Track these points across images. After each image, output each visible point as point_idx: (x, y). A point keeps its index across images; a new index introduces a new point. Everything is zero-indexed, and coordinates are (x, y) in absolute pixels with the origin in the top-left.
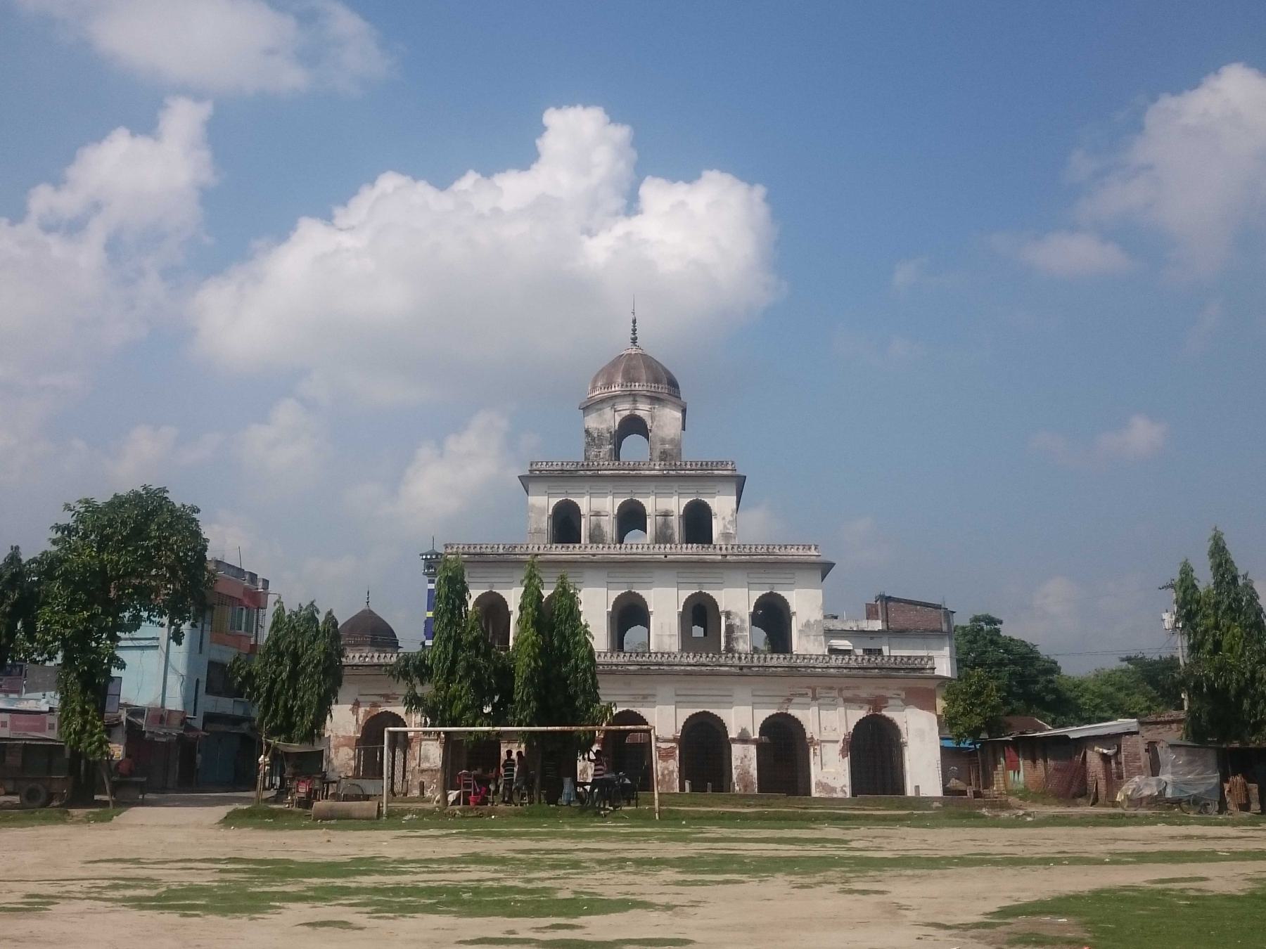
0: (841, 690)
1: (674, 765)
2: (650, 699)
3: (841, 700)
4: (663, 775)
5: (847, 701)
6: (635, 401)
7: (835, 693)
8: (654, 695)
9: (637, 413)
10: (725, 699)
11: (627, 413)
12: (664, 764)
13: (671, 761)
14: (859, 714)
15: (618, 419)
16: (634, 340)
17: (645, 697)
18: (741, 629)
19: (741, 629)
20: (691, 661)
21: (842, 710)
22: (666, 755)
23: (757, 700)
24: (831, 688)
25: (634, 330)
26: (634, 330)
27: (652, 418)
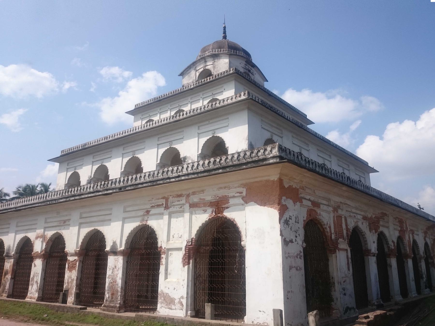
0: (188, 196)
2: (67, 223)
5: (193, 206)
6: (206, 62)
8: (69, 220)
9: (207, 68)
11: (202, 69)
15: (198, 74)
16: (225, 37)
21: (187, 215)
23: (127, 215)
24: (180, 196)
25: (225, 33)
26: (225, 33)
27: (214, 67)
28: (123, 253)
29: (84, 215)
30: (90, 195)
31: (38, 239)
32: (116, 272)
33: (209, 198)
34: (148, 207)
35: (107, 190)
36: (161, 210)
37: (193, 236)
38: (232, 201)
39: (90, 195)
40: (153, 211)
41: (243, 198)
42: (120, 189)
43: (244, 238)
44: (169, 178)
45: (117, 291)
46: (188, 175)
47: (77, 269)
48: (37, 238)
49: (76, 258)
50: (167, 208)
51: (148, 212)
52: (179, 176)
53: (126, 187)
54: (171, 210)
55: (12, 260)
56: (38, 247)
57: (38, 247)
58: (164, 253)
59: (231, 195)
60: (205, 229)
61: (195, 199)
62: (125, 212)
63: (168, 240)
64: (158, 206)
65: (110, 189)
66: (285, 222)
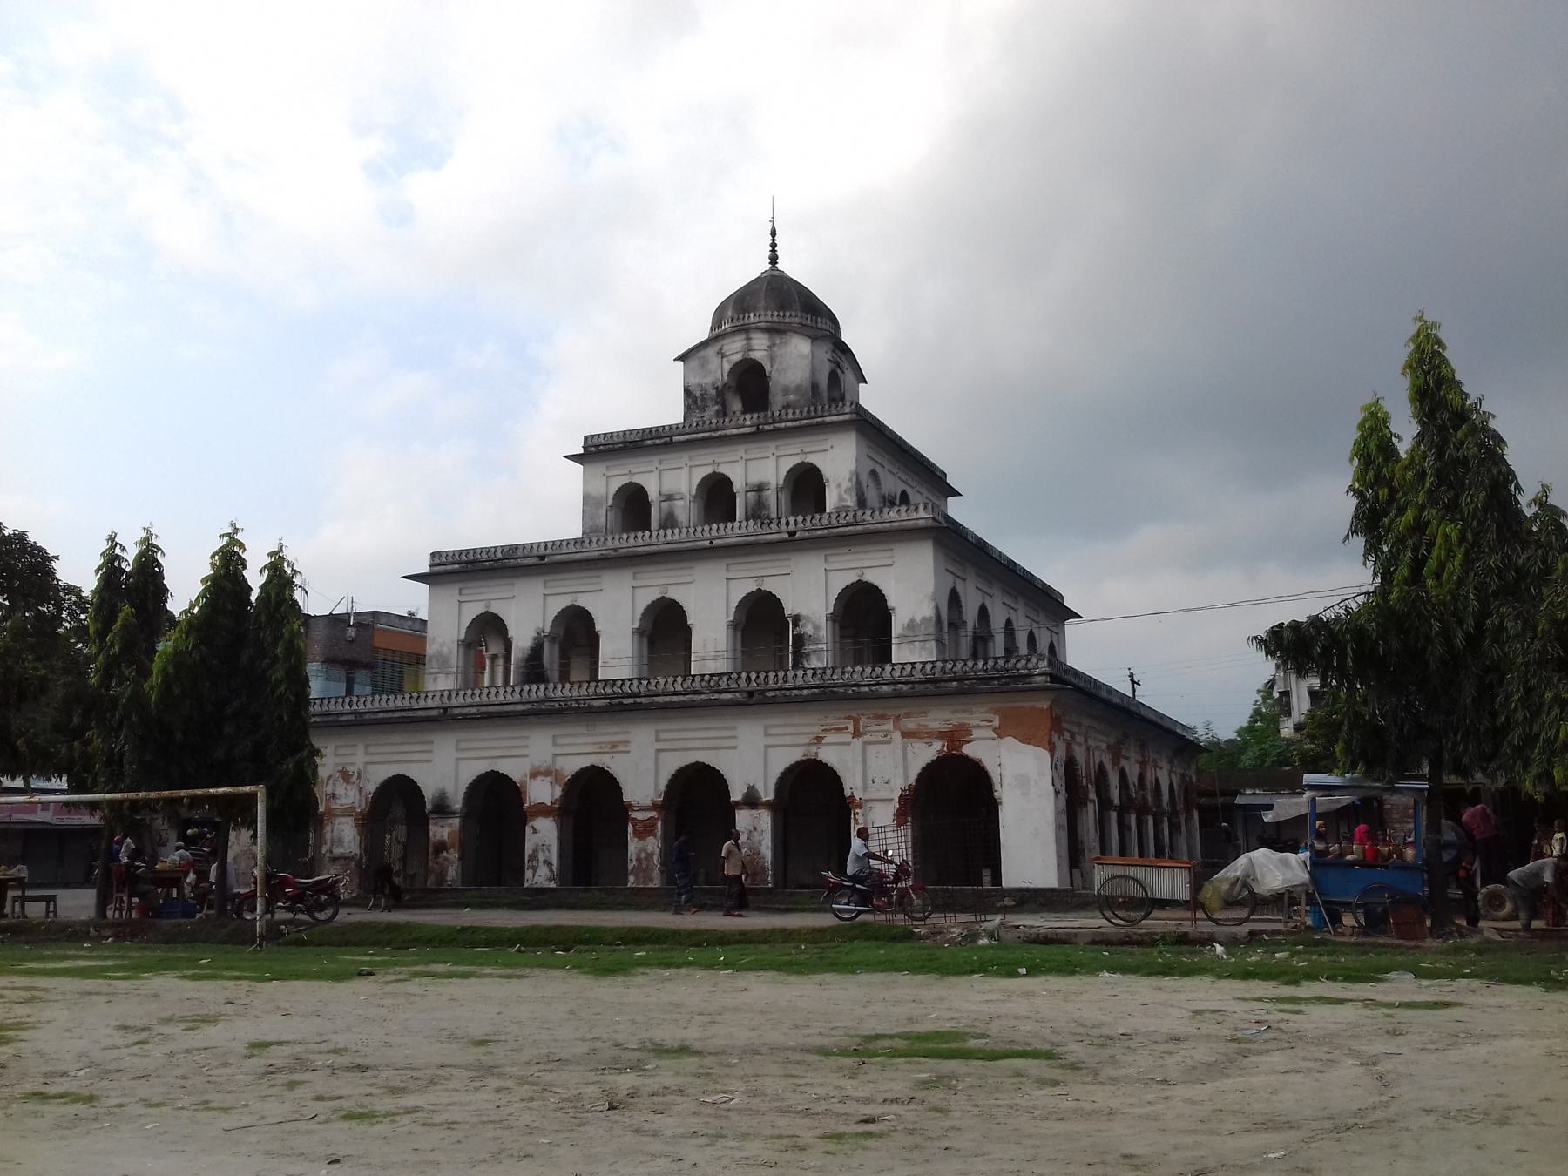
0: (897, 718)
1: (653, 844)
3: (897, 735)
4: (638, 859)
7: (889, 725)
8: (627, 743)
10: (726, 743)
12: (641, 844)
13: (651, 839)
14: (925, 753)
17: (614, 745)
18: (817, 641)
19: (817, 641)
20: (679, 688)
22: (645, 830)
24: (883, 717)
28: (768, 805)
29: (663, 736)
30: (675, 699)
31: (539, 778)
32: (756, 837)
33: (935, 725)
34: (817, 729)
35: (720, 692)
36: (847, 737)
37: (912, 780)
38: (976, 733)
39: (675, 699)
40: (829, 738)
41: (995, 730)
42: (751, 694)
43: (997, 786)
44: (857, 685)
45: (764, 869)
46: (896, 683)
47: (659, 834)
48: (534, 775)
49: (654, 814)
50: (856, 734)
51: (819, 739)
52: (878, 684)
53: (763, 692)
54: (866, 738)
55: (457, 821)
56: (542, 792)
57: (542, 792)
58: (860, 806)
59: (975, 722)
60: (930, 772)
61: (910, 724)
62: (766, 735)
63: (865, 788)
64: (838, 730)
65: (726, 691)
66: (1053, 766)
